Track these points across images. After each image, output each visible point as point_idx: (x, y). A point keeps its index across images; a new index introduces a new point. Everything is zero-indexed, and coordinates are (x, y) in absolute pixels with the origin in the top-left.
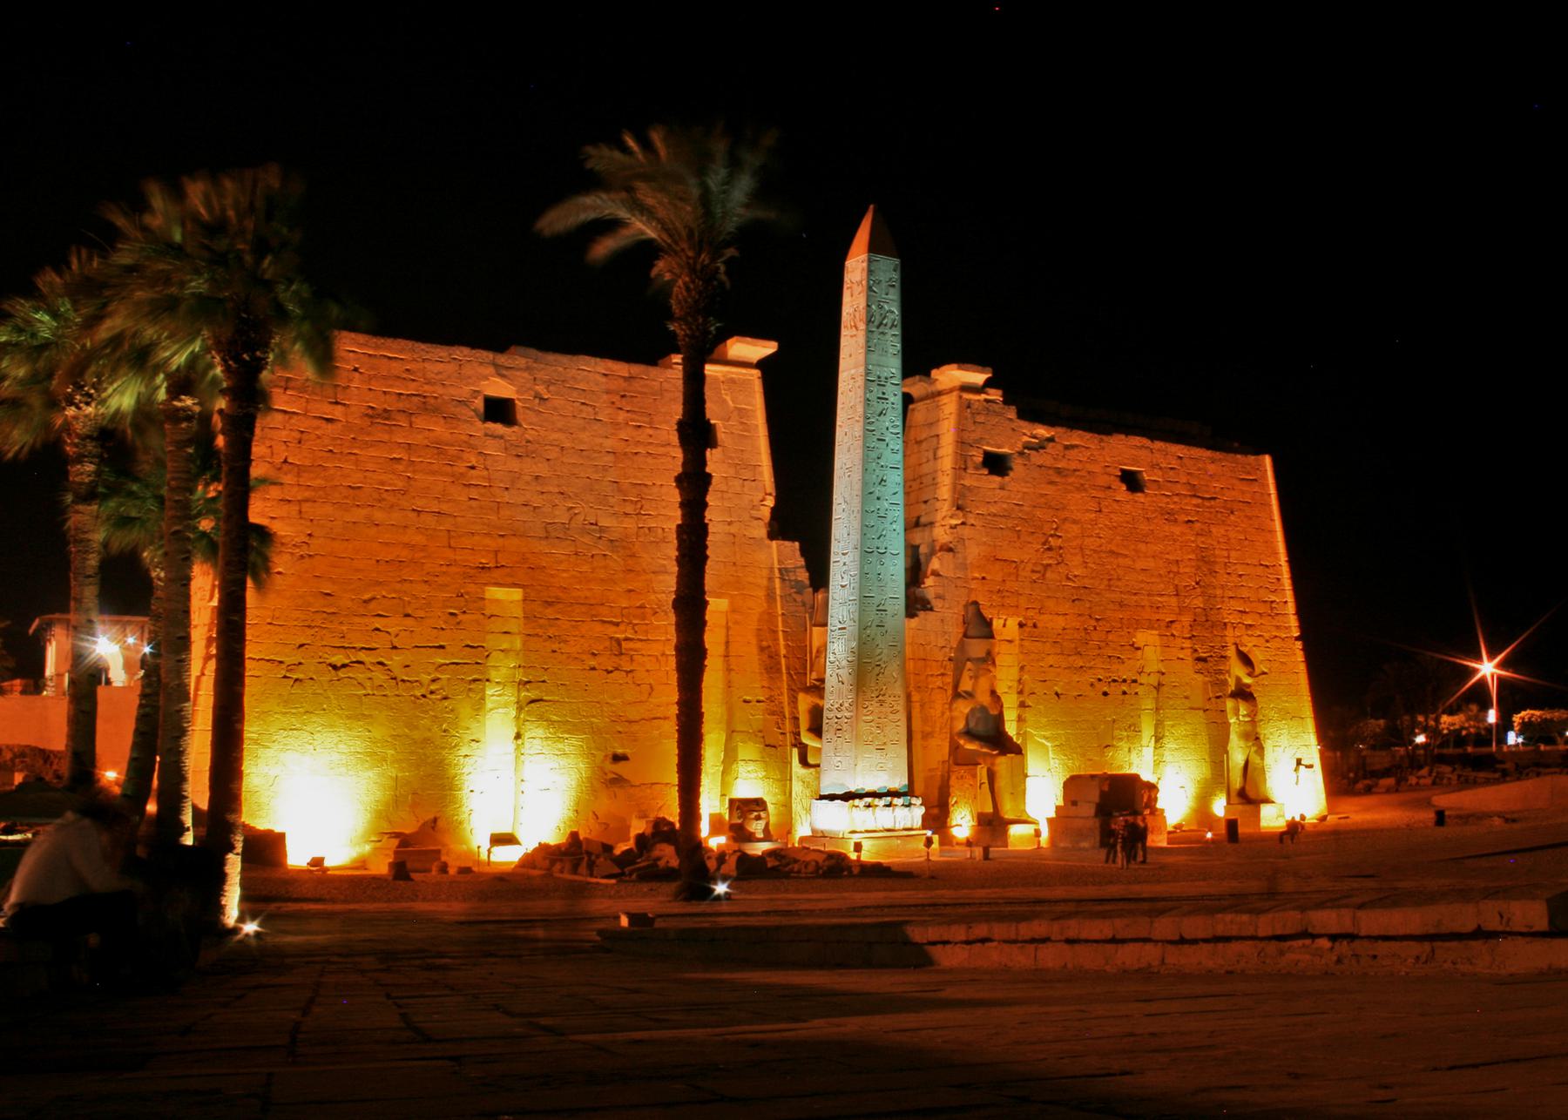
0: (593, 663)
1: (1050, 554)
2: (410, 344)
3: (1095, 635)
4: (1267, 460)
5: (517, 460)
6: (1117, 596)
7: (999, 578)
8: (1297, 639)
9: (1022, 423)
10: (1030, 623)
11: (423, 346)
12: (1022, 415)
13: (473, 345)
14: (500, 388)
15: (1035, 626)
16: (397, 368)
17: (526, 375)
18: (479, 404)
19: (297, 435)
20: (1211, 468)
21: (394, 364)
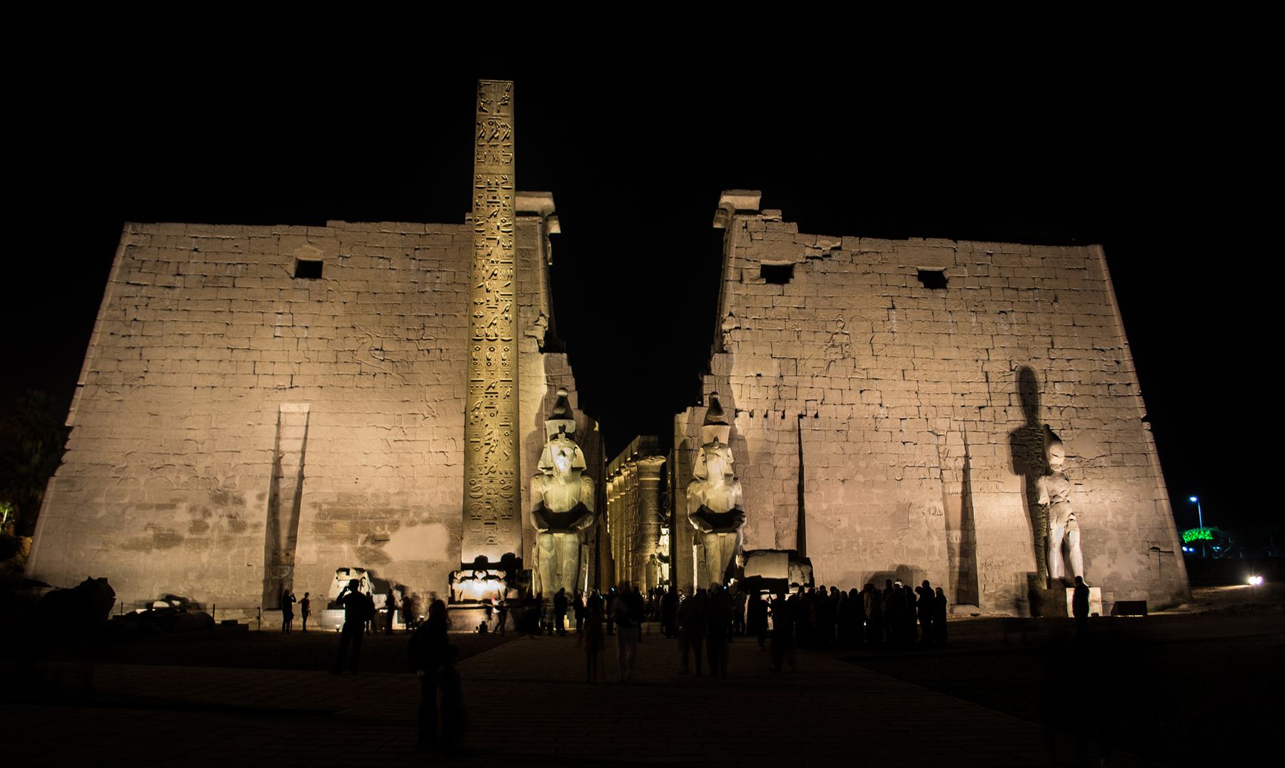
0: (364, 461)
1: (834, 350)
2: (240, 227)
3: (887, 423)
4: (1098, 250)
5: (319, 305)
6: (913, 386)
7: (775, 373)
8: (1144, 420)
9: (803, 236)
10: (811, 414)
11: (250, 228)
12: (802, 230)
13: (291, 223)
14: (310, 253)
15: (816, 416)
16: (228, 246)
17: (334, 240)
18: (291, 268)
19: (145, 300)
20: (1028, 261)
21: (226, 242)
